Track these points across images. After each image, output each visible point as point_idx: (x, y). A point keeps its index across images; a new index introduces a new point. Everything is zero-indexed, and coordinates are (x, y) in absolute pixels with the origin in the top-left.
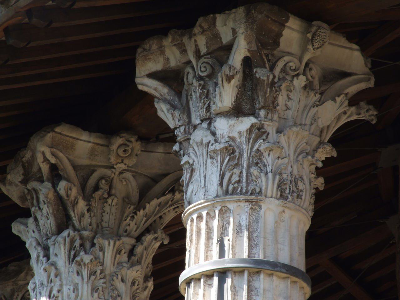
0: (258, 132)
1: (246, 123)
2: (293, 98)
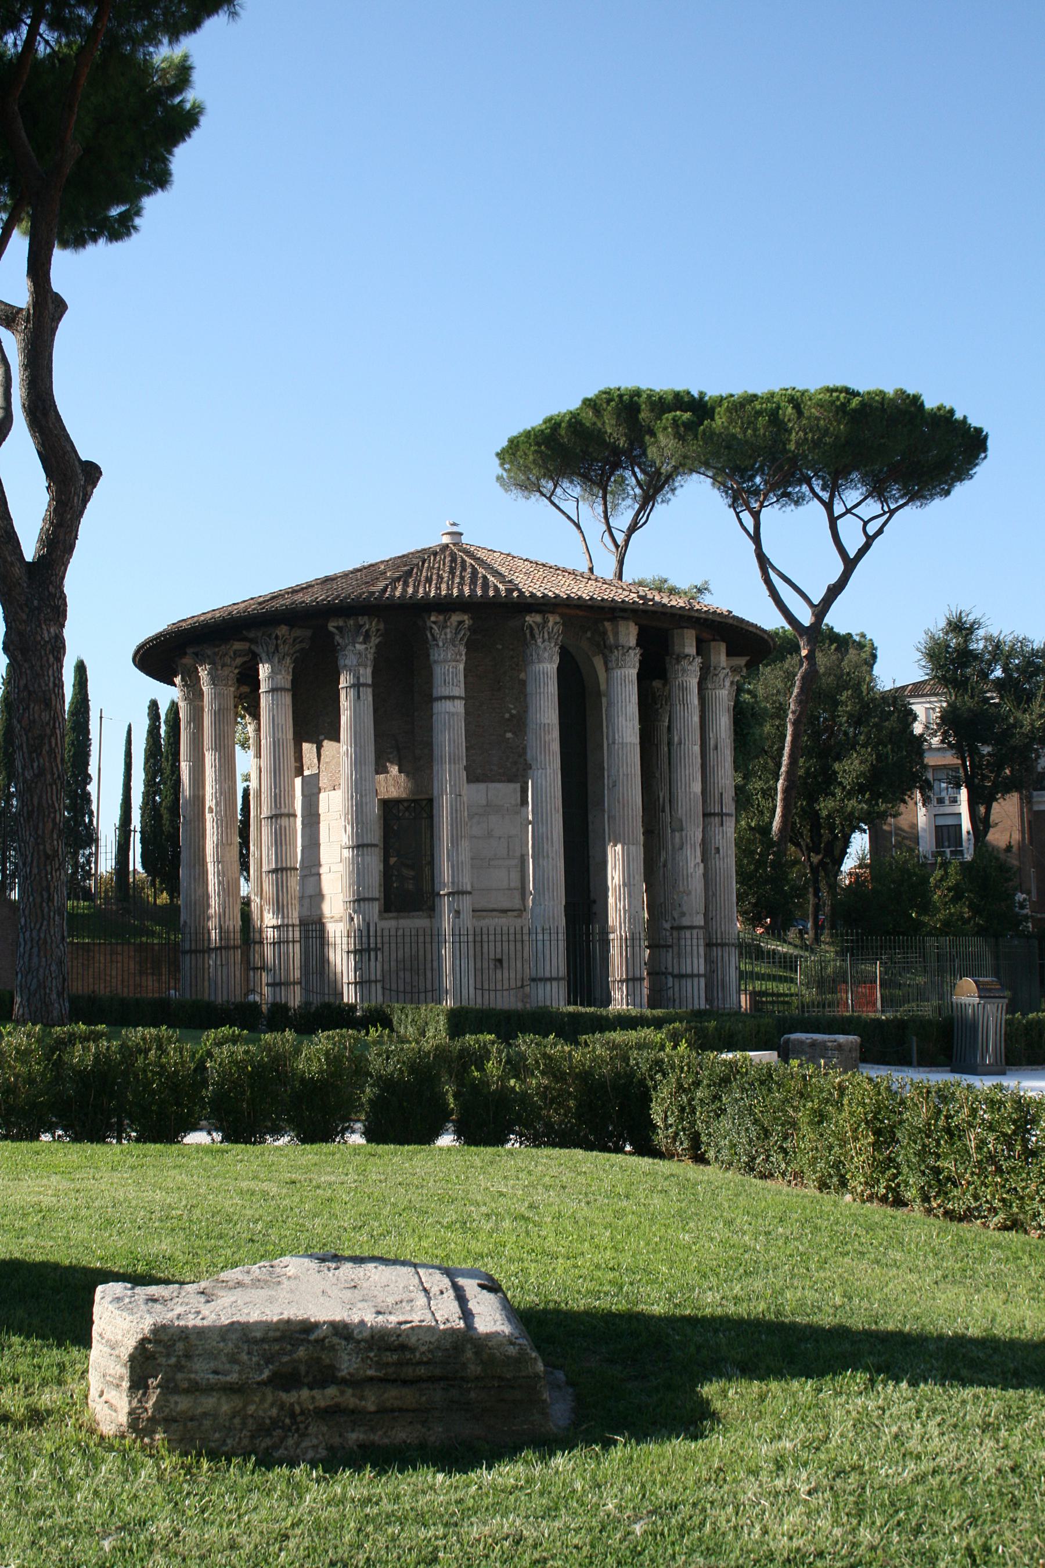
0: (367, 649)
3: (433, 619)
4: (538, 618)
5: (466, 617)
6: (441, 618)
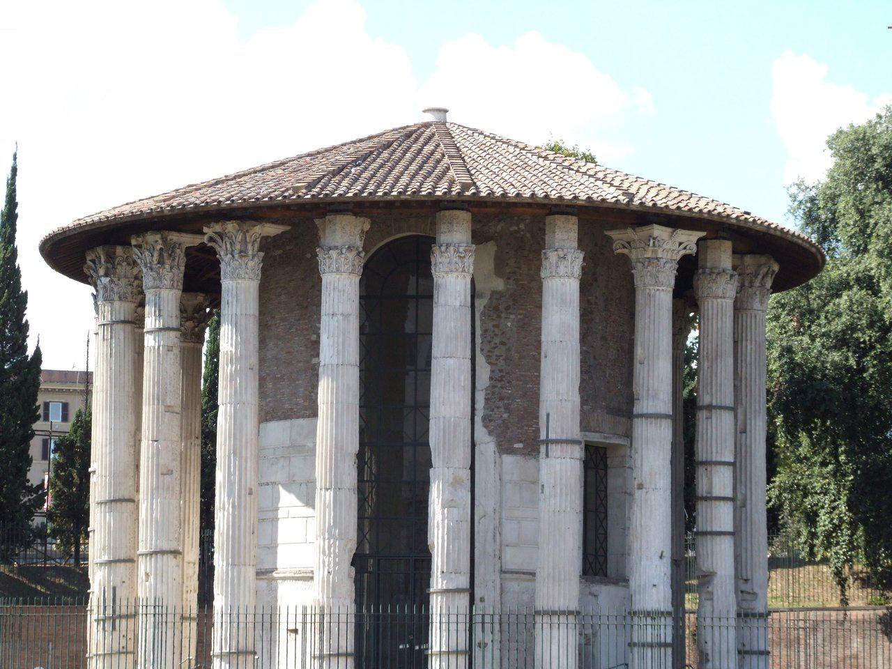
0: (112, 281)
1: (108, 279)
2: (122, 269)
3: (133, 242)
4: (218, 227)
5: (158, 237)
6: (140, 239)
